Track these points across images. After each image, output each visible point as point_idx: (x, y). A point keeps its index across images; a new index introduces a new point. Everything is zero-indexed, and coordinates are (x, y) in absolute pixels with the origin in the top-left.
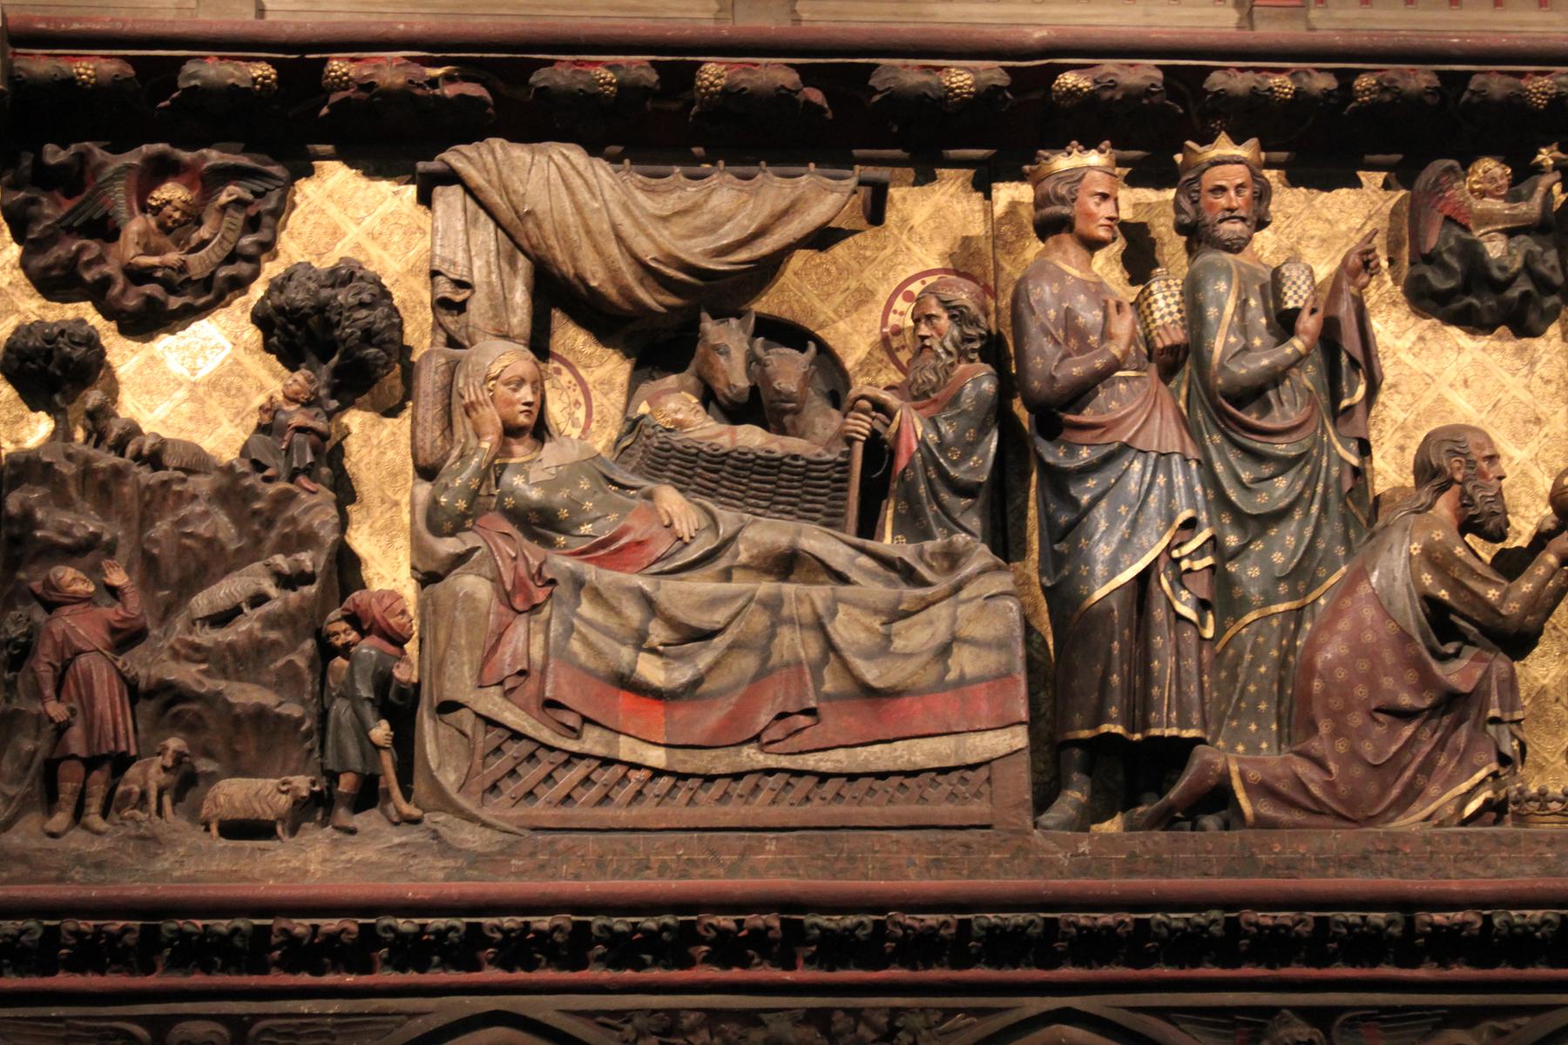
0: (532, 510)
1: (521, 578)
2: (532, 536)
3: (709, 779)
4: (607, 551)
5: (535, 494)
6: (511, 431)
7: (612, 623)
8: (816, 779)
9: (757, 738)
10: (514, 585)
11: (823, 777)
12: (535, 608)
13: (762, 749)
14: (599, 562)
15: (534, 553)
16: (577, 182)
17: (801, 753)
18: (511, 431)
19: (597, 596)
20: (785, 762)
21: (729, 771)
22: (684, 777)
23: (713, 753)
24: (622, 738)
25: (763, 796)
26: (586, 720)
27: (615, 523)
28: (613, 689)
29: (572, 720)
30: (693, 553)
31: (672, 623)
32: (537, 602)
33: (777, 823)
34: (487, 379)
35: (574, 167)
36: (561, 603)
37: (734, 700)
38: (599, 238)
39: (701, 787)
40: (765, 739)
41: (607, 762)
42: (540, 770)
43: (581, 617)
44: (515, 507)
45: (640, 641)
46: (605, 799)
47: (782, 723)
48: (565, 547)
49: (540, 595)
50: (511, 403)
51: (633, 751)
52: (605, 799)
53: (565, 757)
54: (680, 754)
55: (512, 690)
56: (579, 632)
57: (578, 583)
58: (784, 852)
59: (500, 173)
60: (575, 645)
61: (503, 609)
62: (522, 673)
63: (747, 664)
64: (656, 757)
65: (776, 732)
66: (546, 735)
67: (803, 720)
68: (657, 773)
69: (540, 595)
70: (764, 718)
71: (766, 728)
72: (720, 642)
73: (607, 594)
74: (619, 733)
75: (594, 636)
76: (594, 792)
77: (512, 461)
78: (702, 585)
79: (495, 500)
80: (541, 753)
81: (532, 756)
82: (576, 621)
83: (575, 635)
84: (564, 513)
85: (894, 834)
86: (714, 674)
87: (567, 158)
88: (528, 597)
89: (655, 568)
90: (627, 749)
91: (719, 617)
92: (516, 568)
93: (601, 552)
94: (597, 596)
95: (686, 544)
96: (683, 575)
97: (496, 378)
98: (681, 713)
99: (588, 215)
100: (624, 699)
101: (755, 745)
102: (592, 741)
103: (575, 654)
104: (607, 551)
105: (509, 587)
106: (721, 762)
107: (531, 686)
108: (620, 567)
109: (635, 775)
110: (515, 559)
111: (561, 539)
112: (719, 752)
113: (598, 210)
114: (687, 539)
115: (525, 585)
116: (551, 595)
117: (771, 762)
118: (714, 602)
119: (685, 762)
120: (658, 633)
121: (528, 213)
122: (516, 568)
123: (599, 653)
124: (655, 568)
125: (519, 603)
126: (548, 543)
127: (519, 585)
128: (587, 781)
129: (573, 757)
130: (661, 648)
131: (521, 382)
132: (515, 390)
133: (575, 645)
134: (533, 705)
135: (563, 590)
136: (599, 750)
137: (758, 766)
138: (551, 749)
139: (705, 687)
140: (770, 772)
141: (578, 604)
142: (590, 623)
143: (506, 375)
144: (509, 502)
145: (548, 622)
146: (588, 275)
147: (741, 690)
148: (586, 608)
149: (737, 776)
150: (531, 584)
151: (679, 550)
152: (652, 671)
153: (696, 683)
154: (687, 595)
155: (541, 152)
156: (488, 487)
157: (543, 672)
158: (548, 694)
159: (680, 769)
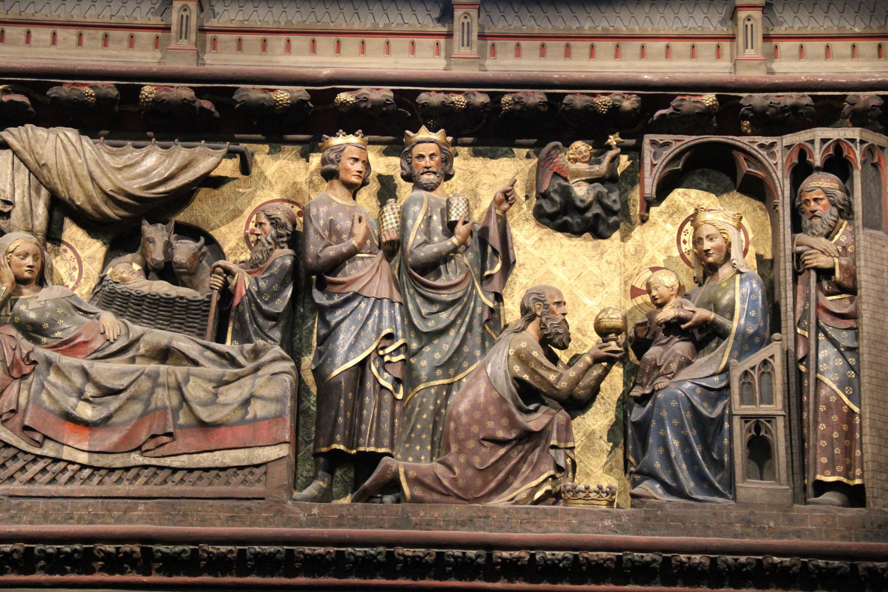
0: (28, 323)
1: (17, 360)
2: (29, 338)
3: (111, 470)
4: (68, 346)
5: (32, 316)
6: (20, 281)
7: (66, 385)
8: (170, 471)
9: (139, 448)
10: (12, 363)
11: (175, 470)
12: (24, 377)
13: (143, 453)
14: (63, 352)
15: (26, 345)
16: (70, 148)
17: (163, 457)
18: (20, 281)
19: (59, 370)
20: (154, 462)
21: (122, 466)
22: (98, 469)
23: (115, 456)
24: (65, 447)
25: (142, 479)
26: (46, 437)
27: (74, 331)
28: (62, 421)
29: (38, 437)
30: (115, 347)
31: (97, 385)
32: (24, 373)
33: (146, 494)
34: (7, 253)
35: (70, 140)
36: (38, 374)
37: (128, 427)
38: (82, 179)
39: (107, 474)
40: (144, 449)
41: (56, 460)
42: (19, 464)
43: (49, 382)
44: (20, 322)
45: (80, 394)
46: (53, 481)
47: (154, 440)
48: (46, 344)
49: (27, 369)
50: (20, 266)
51: (70, 454)
52: (53, 481)
53: (33, 457)
54: (96, 456)
55: (6, 420)
56: (47, 390)
57: (49, 363)
58: (148, 511)
59: (30, 143)
60: (44, 397)
61: (5, 376)
62: (13, 411)
63: (137, 408)
64: (83, 458)
65: (150, 445)
66: (23, 445)
67: (165, 439)
68: (83, 467)
69: (27, 369)
70: (144, 437)
71: (145, 443)
72: (123, 396)
73: (64, 370)
74: (63, 444)
75: (53, 392)
76: (48, 477)
77: (22, 297)
78: (117, 365)
79: (9, 318)
80: (20, 455)
81: (14, 457)
82: (46, 384)
83: (44, 391)
84: (46, 326)
85: (210, 502)
86: (119, 413)
87: (66, 135)
88: (20, 370)
89: (94, 356)
90: (67, 454)
91: (125, 382)
92: (14, 354)
93: (64, 347)
94: (59, 370)
95: (112, 343)
96: (109, 360)
97: (12, 252)
98: (99, 434)
99: (76, 166)
100: (68, 426)
101: (138, 452)
102: (49, 450)
103: (44, 402)
104: (68, 346)
105: (8, 365)
106: (118, 461)
107: (17, 419)
108: (74, 355)
109: (70, 467)
110: (14, 349)
111: (44, 340)
112: (118, 455)
113: (81, 164)
114: (112, 340)
115: (19, 364)
116: (34, 369)
117: (146, 461)
118: (124, 374)
119: (98, 461)
120: (90, 391)
121: (44, 165)
122: (14, 354)
123: (55, 401)
124: (94, 356)
125: (15, 373)
126: (37, 342)
127: (15, 364)
128: (44, 471)
129: (37, 458)
130: (91, 399)
131: (26, 255)
132: (23, 259)
133: (44, 397)
134: (18, 429)
135: (41, 367)
136: (52, 454)
137: (139, 464)
138: (26, 453)
139: (114, 420)
140: (146, 467)
141: (48, 374)
142: (54, 385)
143: (18, 251)
144: (17, 319)
145: (31, 384)
146: (75, 199)
147: (133, 422)
148: (52, 377)
149: (127, 469)
150: (22, 363)
151: (107, 347)
152: (86, 412)
153: (109, 417)
154: (108, 371)
155: (53, 132)
156: (6, 311)
157: (25, 411)
158: (26, 423)
159: (95, 464)
